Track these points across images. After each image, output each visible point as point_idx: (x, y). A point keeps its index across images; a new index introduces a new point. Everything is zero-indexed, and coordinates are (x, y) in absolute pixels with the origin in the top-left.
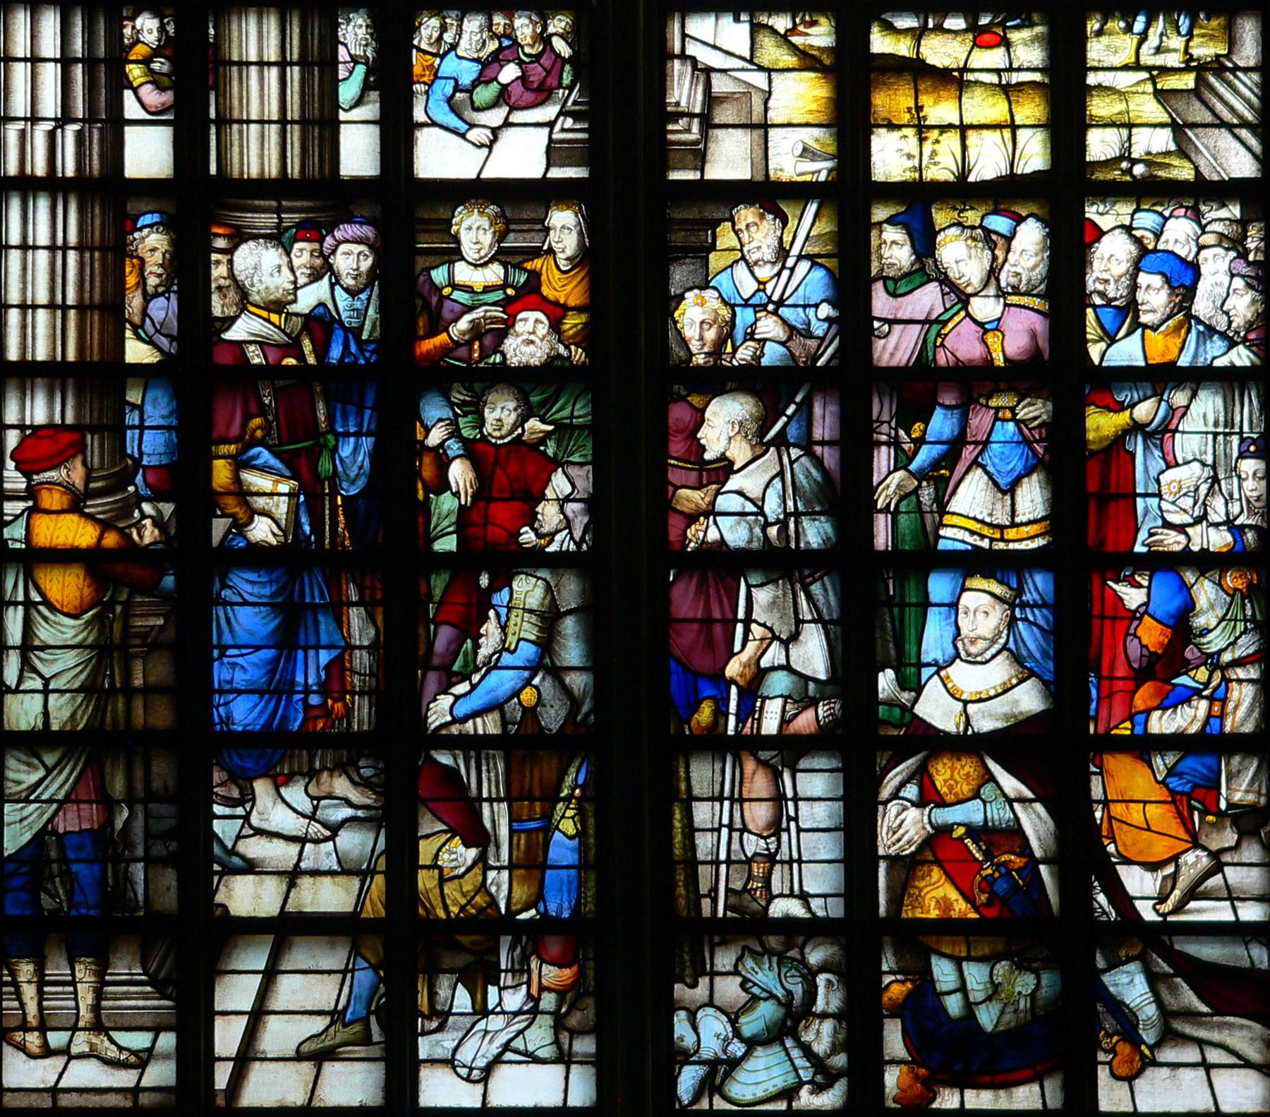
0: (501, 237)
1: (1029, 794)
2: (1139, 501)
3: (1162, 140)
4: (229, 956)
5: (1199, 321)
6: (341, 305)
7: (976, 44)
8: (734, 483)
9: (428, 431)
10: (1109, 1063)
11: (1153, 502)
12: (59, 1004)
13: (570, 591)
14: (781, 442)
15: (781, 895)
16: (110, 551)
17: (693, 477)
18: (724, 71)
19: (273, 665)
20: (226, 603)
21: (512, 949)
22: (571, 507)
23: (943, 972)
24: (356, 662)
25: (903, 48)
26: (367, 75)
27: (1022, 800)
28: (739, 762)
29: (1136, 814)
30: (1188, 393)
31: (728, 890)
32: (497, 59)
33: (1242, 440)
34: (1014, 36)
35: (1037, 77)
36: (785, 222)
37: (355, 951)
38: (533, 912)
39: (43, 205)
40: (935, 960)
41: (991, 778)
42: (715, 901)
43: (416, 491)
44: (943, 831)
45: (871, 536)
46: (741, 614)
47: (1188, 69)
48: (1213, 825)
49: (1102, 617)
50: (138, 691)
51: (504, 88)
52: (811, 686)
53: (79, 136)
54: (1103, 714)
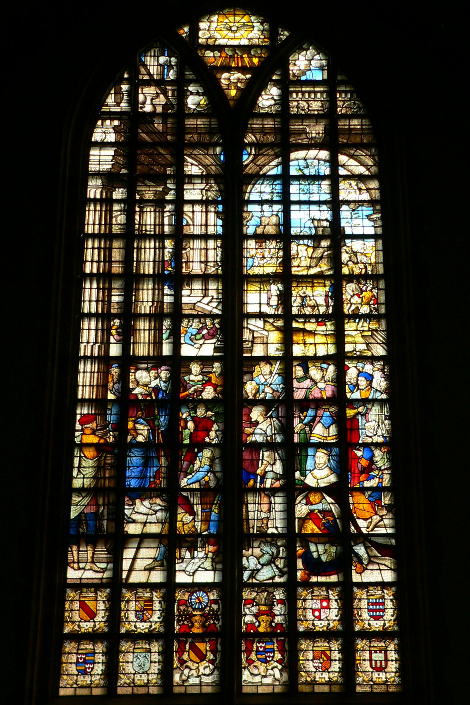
0: (202, 369)
1: (333, 502)
2: (360, 431)
3: (364, 347)
4: (128, 544)
5: (374, 388)
6: (162, 385)
7: (318, 325)
8: (259, 427)
9: (182, 414)
10: (355, 569)
11: (364, 431)
12: (83, 556)
13: (217, 453)
14: (271, 417)
15: (271, 528)
16: (101, 444)
17: (249, 425)
18: (257, 331)
19: (142, 471)
20: (130, 456)
21: (201, 542)
22: (218, 433)
23: (313, 547)
24: (163, 471)
25: (300, 326)
26: (170, 332)
27: (332, 503)
28: (260, 495)
29: (361, 506)
30: (371, 405)
31: (257, 526)
32: (202, 329)
33: (385, 416)
34: (327, 323)
35: (333, 332)
36: (272, 365)
37: (160, 543)
38: (206, 532)
39: (89, 362)
40: (310, 543)
41: (324, 498)
42: (254, 529)
43: (179, 429)
44: (312, 511)
45: (293, 439)
46: (261, 458)
47: (369, 331)
48: (380, 509)
49: (352, 458)
50: (107, 478)
51: (203, 335)
52: (278, 475)
53: (99, 347)
54: (352, 482)
